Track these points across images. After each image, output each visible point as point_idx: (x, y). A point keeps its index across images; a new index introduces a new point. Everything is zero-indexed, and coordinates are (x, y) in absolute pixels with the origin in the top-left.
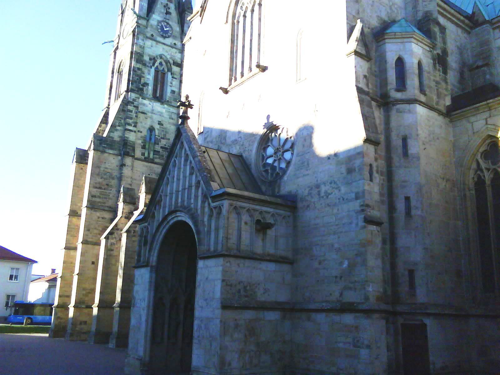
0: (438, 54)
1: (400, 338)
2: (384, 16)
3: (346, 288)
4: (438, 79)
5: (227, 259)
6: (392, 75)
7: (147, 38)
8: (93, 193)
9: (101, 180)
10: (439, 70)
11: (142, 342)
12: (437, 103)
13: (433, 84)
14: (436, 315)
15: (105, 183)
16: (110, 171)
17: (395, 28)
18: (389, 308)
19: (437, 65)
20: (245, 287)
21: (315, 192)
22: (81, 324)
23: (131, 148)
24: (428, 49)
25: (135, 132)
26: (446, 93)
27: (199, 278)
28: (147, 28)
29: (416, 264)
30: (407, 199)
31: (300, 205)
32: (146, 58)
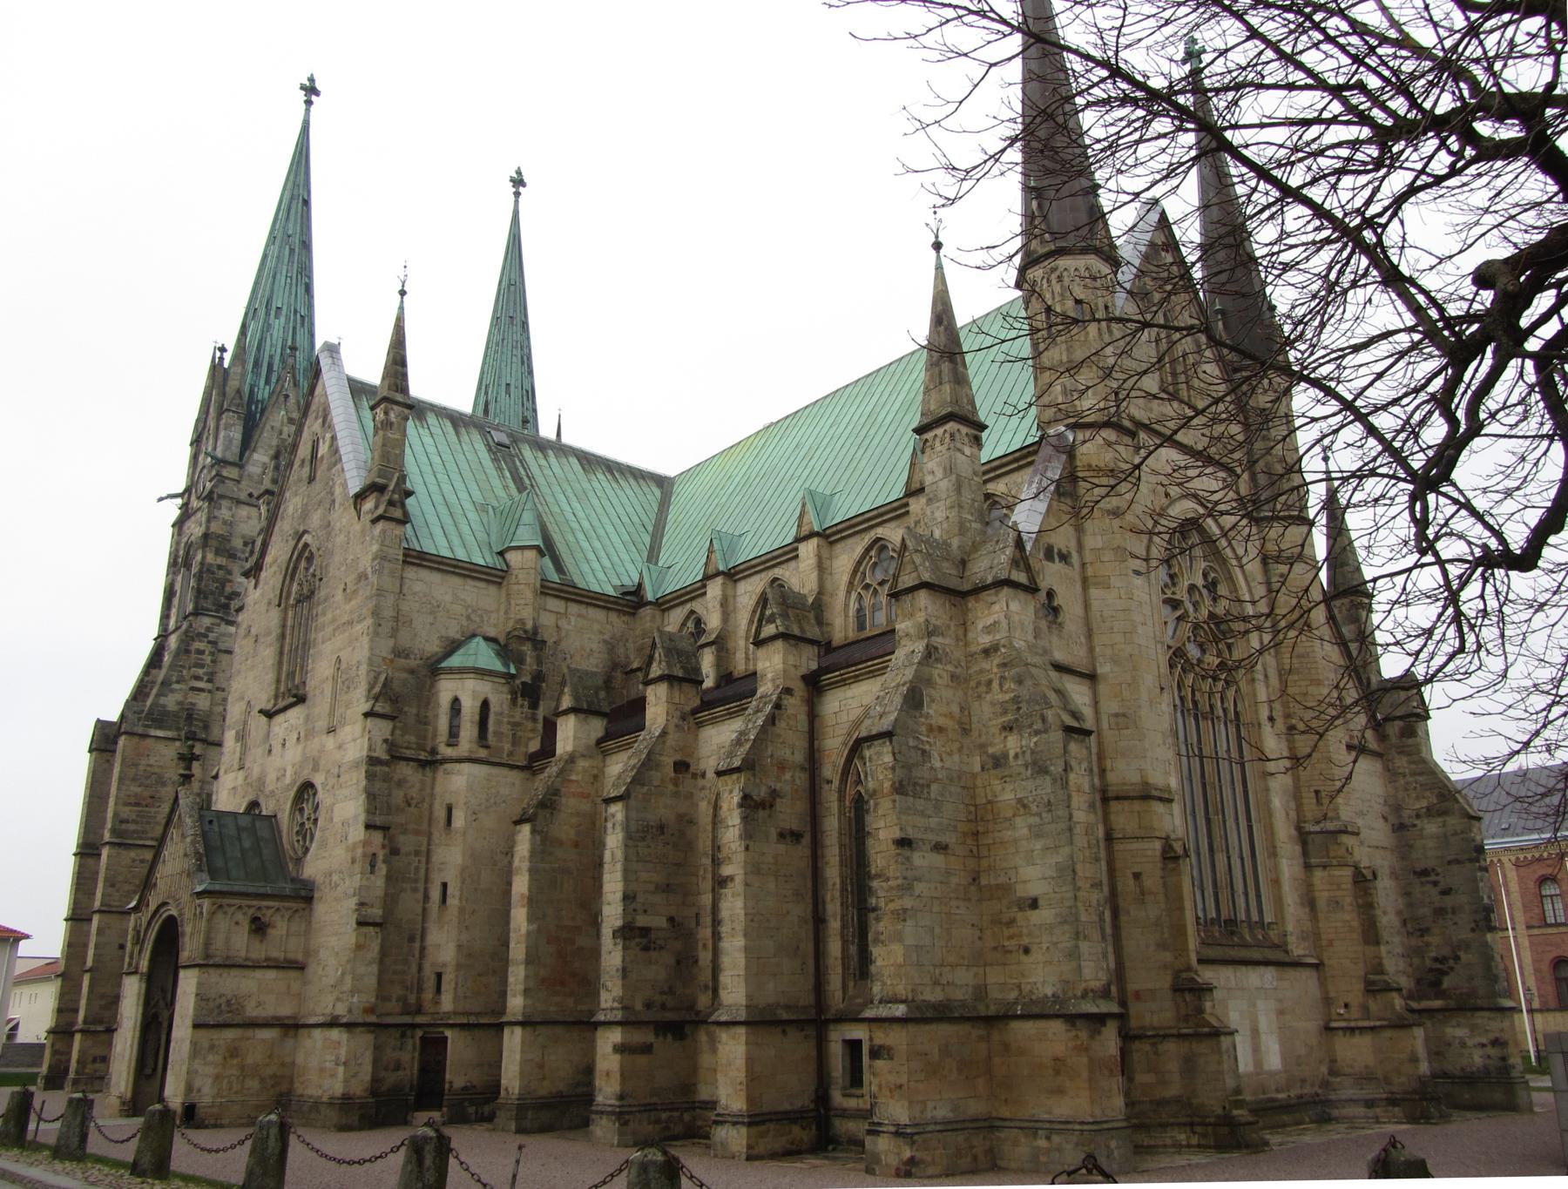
0: (524, 684)
1: (417, 1054)
2: (454, 632)
3: (338, 999)
4: (517, 719)
5: (204, 970)
6: (443, 723)
7: (239, 502)
8: (124, 816)
9: (139, 790)
10: (522, 706)
11: (124, 1075)
12: (511, 754)
13: (505, 729)
14: (462, 1026)
15: (146, 794)
16: (156, 770)
17: (455, 661)
18: (407, 1019)
19: (520, 699)
20: (228, 1001)
21: (327, 881)
22: (94, 1060)
23: (201, 724)
24: (503, 681)
25: (210, 691)
26: (531, 735)
27: (179, 991)
28: (238, 482)
29: (444, 965)
30: (445, 885)
31: (316, 895)
32: (237, 543)
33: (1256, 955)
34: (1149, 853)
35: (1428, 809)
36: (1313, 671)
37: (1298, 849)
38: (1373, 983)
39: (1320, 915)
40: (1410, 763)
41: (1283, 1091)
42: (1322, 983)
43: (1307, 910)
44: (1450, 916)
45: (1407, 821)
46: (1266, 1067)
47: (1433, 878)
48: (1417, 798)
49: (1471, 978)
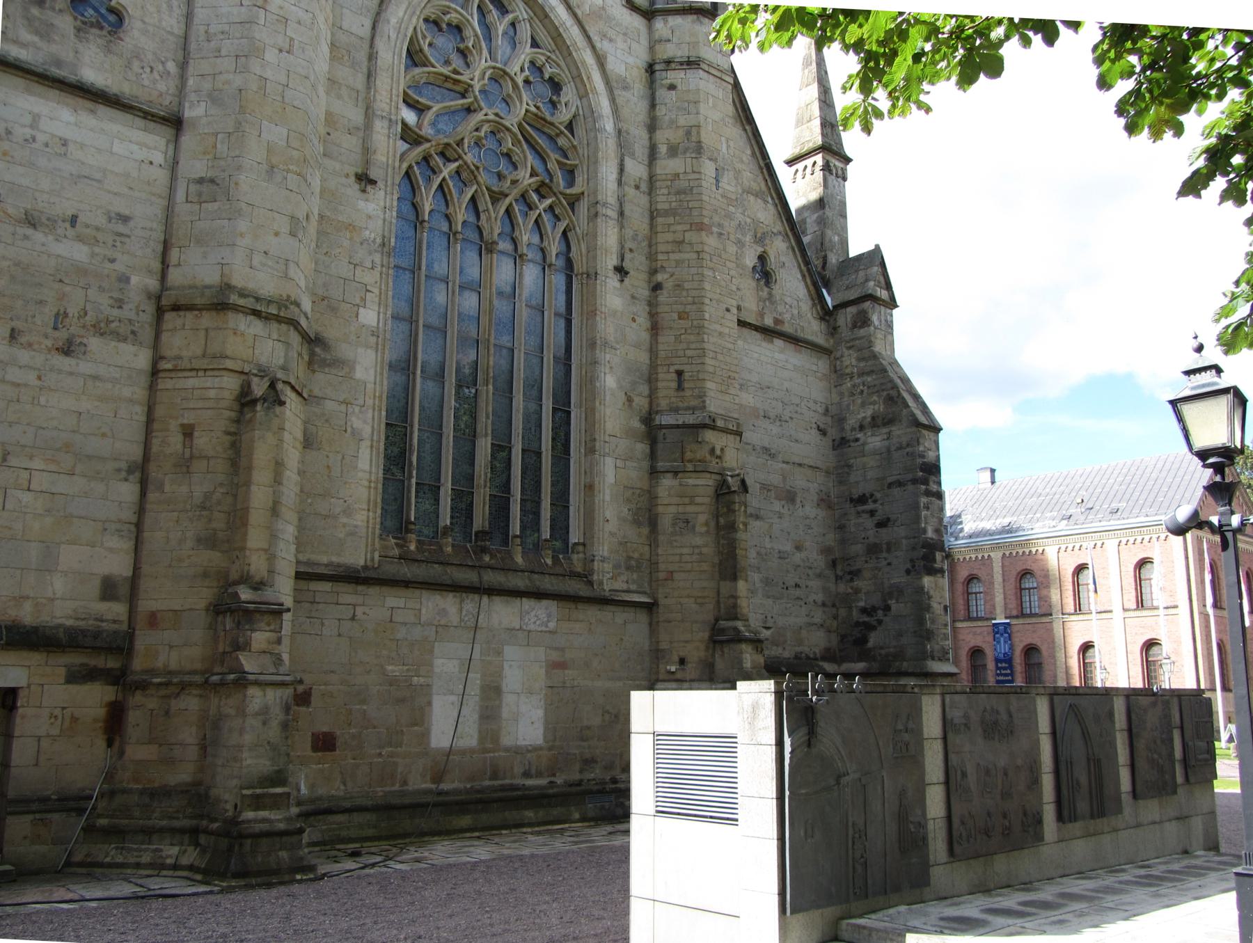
33: (519, 582)
34: (212, 393)
35: (873, 418)
36: (695, 213)
37: (642, 448)
38: (722, 631)
39: (661, 538)
40: (859, 359)
41: (539, 774)
42: (653, 627)
43: (645, 531)
44: (884, 555)
45: (849, 435)
46: (506, 741)
47: (870, 506)
48: (863, 405)
49: (900, 635)
